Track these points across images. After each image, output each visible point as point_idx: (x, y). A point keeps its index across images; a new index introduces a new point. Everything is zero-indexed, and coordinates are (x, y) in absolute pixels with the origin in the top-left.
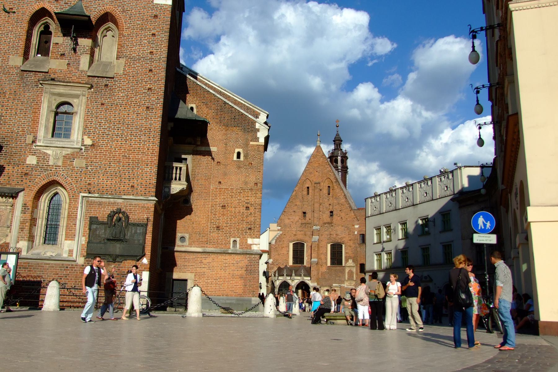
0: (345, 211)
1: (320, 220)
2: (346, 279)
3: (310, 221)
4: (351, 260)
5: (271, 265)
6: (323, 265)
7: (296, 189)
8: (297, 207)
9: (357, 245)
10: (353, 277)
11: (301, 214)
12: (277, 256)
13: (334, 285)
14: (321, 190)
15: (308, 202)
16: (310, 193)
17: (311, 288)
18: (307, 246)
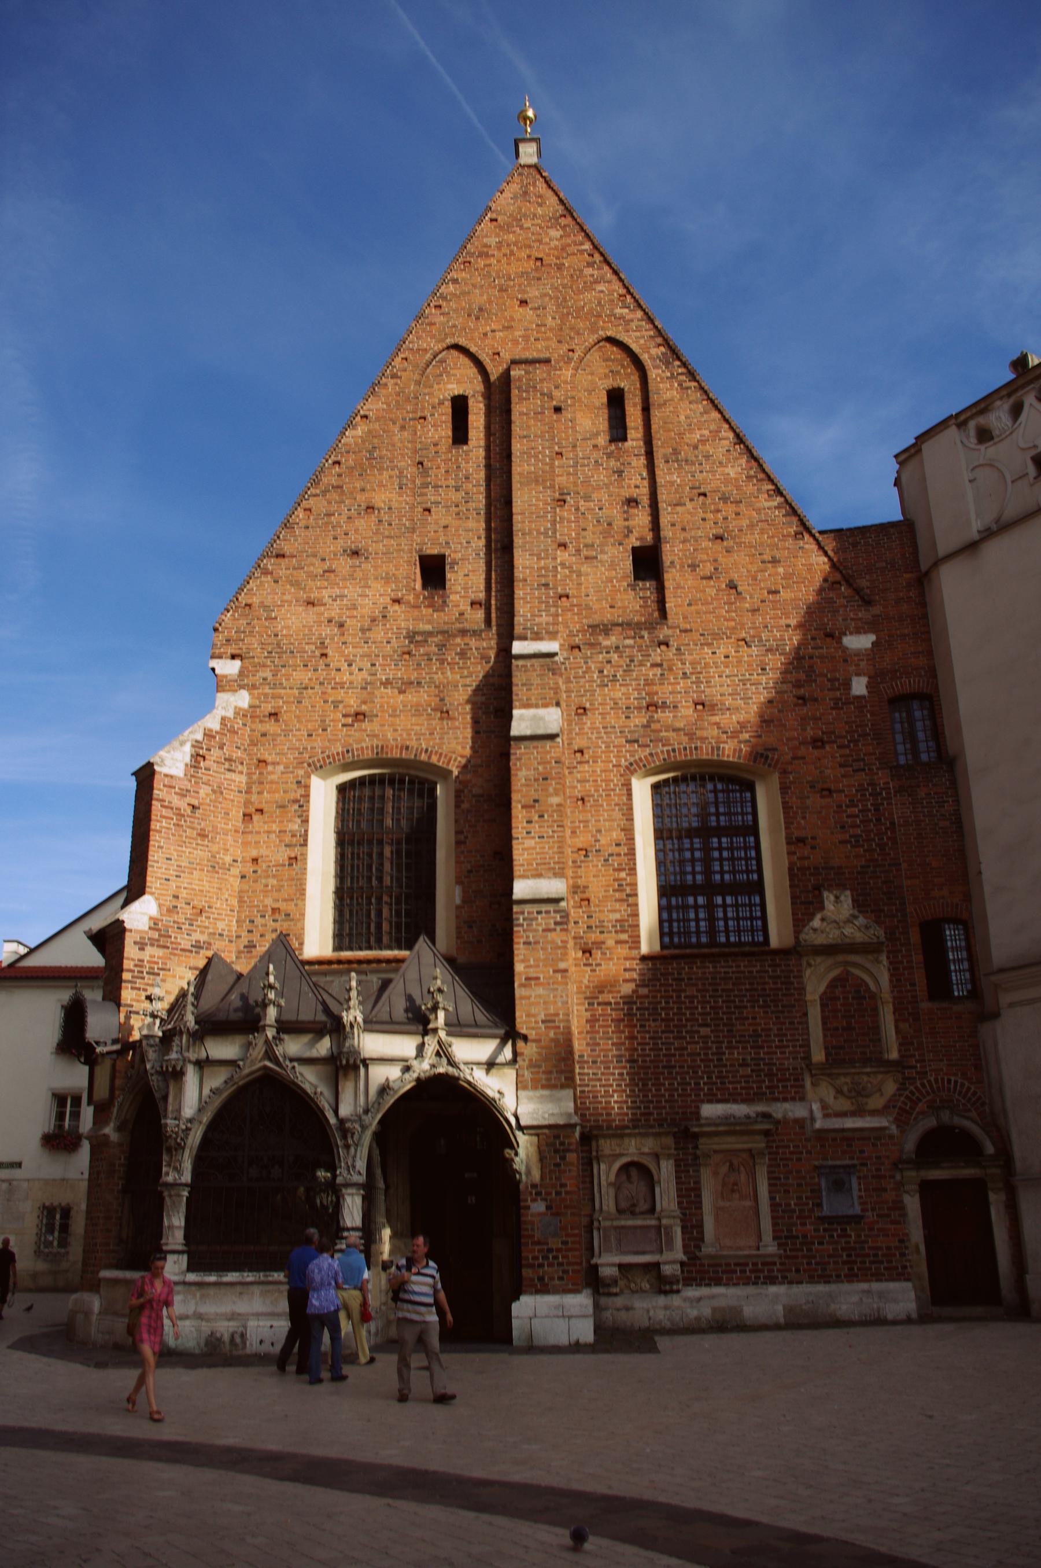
2: (818, 1056)
4: (847, 898)
6: (599, 944)
7: (373, 406)
8: (373, 518)
9: (882, 777)
12: (199, 882)
13: (710, 1110)
14: (558, 410)
17: (522, 1139)
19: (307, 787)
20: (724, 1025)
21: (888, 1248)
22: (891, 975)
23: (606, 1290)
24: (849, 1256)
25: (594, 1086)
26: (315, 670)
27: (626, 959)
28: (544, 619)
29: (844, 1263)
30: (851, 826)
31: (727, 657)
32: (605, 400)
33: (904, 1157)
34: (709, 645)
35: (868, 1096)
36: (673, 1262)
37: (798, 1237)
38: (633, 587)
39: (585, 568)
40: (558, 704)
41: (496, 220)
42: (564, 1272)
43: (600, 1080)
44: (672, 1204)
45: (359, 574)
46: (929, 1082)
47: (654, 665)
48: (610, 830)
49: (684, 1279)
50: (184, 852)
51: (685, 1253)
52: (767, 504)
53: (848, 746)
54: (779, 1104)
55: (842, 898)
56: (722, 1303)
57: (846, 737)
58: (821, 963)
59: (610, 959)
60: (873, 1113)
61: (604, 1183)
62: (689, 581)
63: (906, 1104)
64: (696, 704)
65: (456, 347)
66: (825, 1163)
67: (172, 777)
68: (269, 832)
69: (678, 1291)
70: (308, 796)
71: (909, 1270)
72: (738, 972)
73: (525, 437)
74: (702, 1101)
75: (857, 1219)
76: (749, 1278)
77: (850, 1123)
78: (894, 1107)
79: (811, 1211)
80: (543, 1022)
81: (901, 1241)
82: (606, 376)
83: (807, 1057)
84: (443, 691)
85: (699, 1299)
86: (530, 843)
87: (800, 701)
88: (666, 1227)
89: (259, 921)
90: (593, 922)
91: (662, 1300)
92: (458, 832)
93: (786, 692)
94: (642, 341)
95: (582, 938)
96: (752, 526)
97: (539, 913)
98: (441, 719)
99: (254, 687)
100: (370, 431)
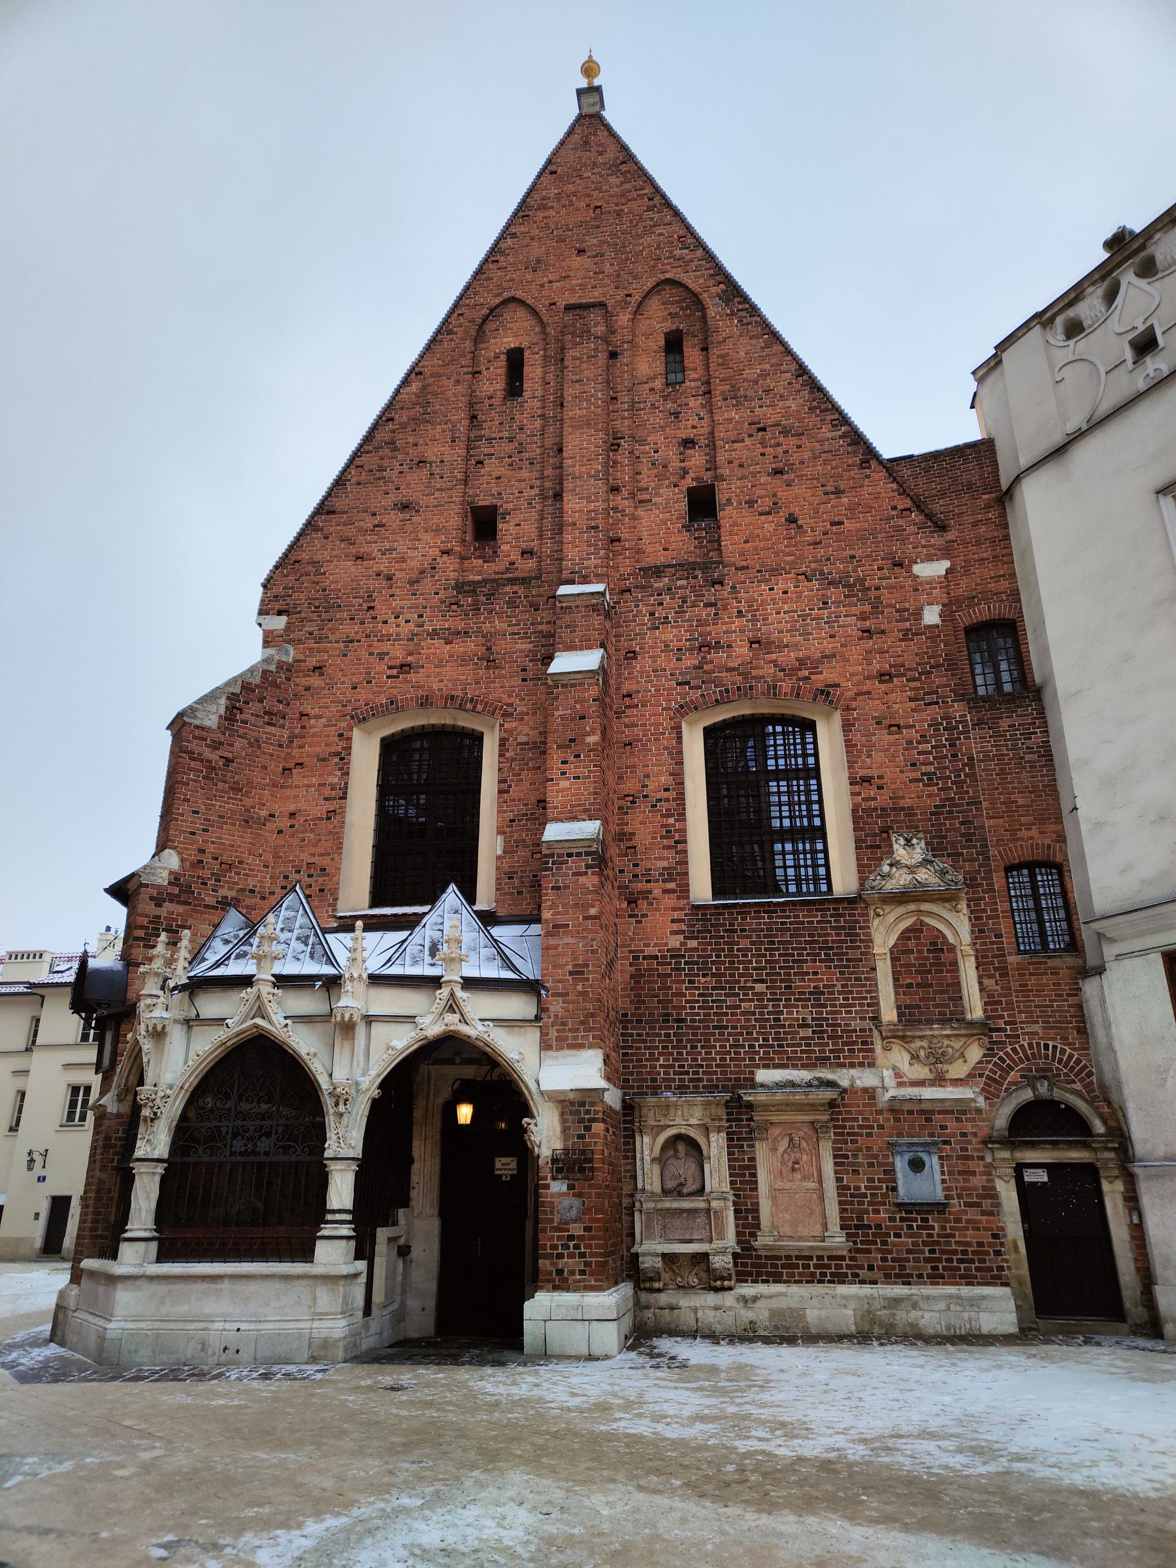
0: (808, 471)
1: (617, 547)
2: (889, 1014)
3: (531, 564)
5: (158, 902)
9: (958, 710)
10: (955, 988)
11: (453, 520)
13: (764, 1076)
15: (511, 440)
16: (527, 385)
18: (503, 743)
19: (350, 739)
20: (782, 981)
21: (980, 1244)
22: (973, 925)
23: (648, 1285)
24: (932, 1251)
25: (637, 1048)
26: (362, 623)
27: (674, 909)
28: (593, 561)
29: (926, 1260)
30: (922, 764)
31: (785, 592)
32: (662, 343)
33: (995, 1134)
34: (766, 581)
35: (950, 1062)
36: (723, 1252)
37: (870, 1227)
38: (687, 528)
39: (640, 512)
40: (602, 646)
41: (555, 172)
42: (587, 1264)
43: (645, 1041)
44: (723, 1184)
45: (409, 527)
46: (1022, 1047)
47: (707, 605)
48: (659, 774)
49: (738, 1273)
50: (214, 805)
51: (739, 1242)
52: (830, 435)
53: (919, 679)
54: (845, 1071)
55: (914, 841)
56: (781, 1303)
57: (916, 669)
58: (893, 913)
59: (657, 910)
60: (956, 1082)
61: (647, 1158)
62: (747, 518)
63: (995, 1073)
64: (751, 643)
65: (513, 300)
66: (901, 1140)
67: (203, 729)
68: (309, 786)
69: (730, 1289)
70: (350, 748)
71: (1006, 1272)
72: (796, 923)
73: (577, 381)
74: (758, 1066)
75: (940, 1208)
76: (813, 1274)
77: (929, 1093)
78: (981, 1076)
79: (885, 1195)
80: (571, 973)
81: (995, 1236)
82: (664, 320)
83: (876, 1019)
84: (489, 641)
85: (755, 1299)
86: (564, 784)
87: (865, 634)
88: (716, 1212)
89: (294, 877)
90: (638, 870)
91: (711, 1299)
92: (500, 782)
93: (850, 625)
94: (701, 281)
95: (627, 887)
96: (815, 457)
97: (570, 855)
98: (488, 668)
99: (300, 641)
100: (424, 387)
